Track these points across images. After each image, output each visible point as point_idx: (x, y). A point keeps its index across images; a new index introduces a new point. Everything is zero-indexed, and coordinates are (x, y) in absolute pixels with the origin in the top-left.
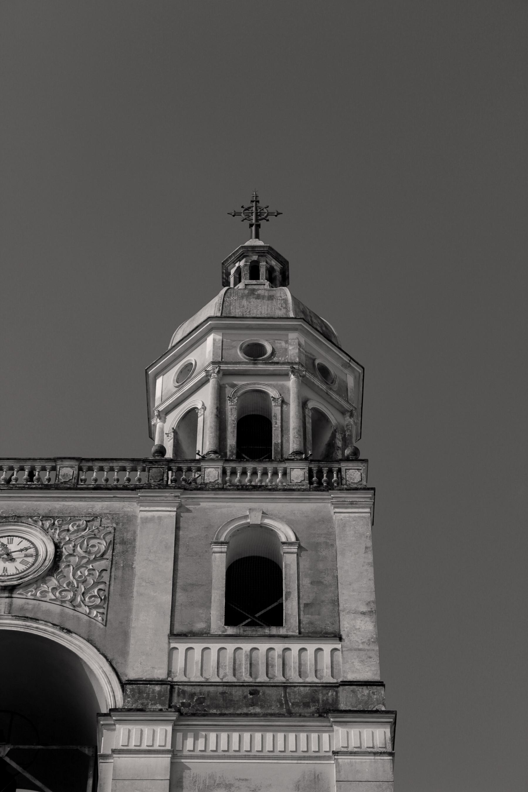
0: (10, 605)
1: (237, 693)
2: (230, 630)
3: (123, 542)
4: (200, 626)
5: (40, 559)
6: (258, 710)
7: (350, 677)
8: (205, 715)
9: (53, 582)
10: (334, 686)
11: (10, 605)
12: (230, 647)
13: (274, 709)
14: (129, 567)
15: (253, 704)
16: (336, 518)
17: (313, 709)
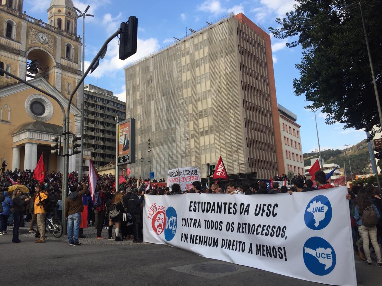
0: (43, 46)
1: (67, 68)
2: (67, 59)
3: (55, 41)
4: (64, 57)
5: (46, 40)
6: (69, 71)
7: (79, 69)
8: (65, 70)
9: (47, 45)
10: (77, 70)
11: (43, 46)
12: (67, 61)
13: (71, 71)
14: (56, 45)
15: (69, 70)
16: (78, 46)
17: (75, 72)
